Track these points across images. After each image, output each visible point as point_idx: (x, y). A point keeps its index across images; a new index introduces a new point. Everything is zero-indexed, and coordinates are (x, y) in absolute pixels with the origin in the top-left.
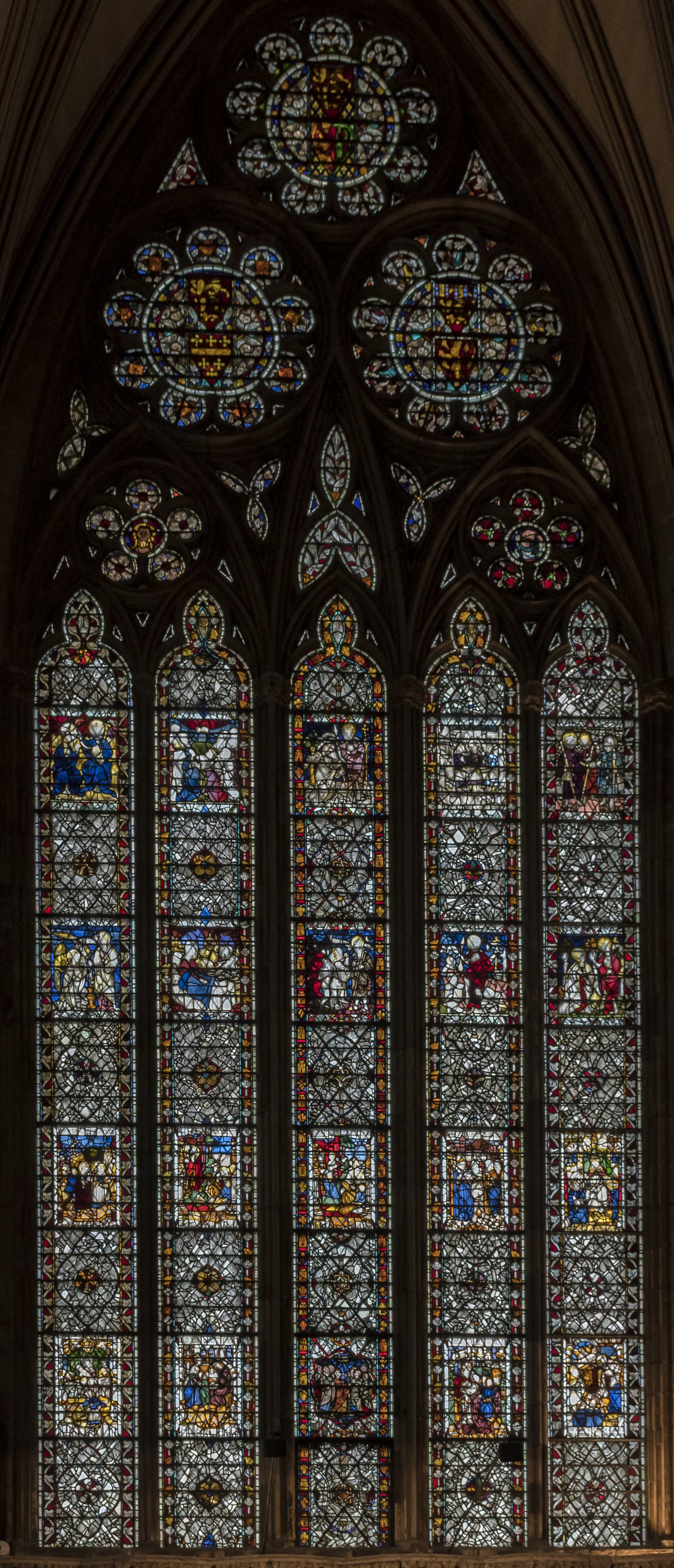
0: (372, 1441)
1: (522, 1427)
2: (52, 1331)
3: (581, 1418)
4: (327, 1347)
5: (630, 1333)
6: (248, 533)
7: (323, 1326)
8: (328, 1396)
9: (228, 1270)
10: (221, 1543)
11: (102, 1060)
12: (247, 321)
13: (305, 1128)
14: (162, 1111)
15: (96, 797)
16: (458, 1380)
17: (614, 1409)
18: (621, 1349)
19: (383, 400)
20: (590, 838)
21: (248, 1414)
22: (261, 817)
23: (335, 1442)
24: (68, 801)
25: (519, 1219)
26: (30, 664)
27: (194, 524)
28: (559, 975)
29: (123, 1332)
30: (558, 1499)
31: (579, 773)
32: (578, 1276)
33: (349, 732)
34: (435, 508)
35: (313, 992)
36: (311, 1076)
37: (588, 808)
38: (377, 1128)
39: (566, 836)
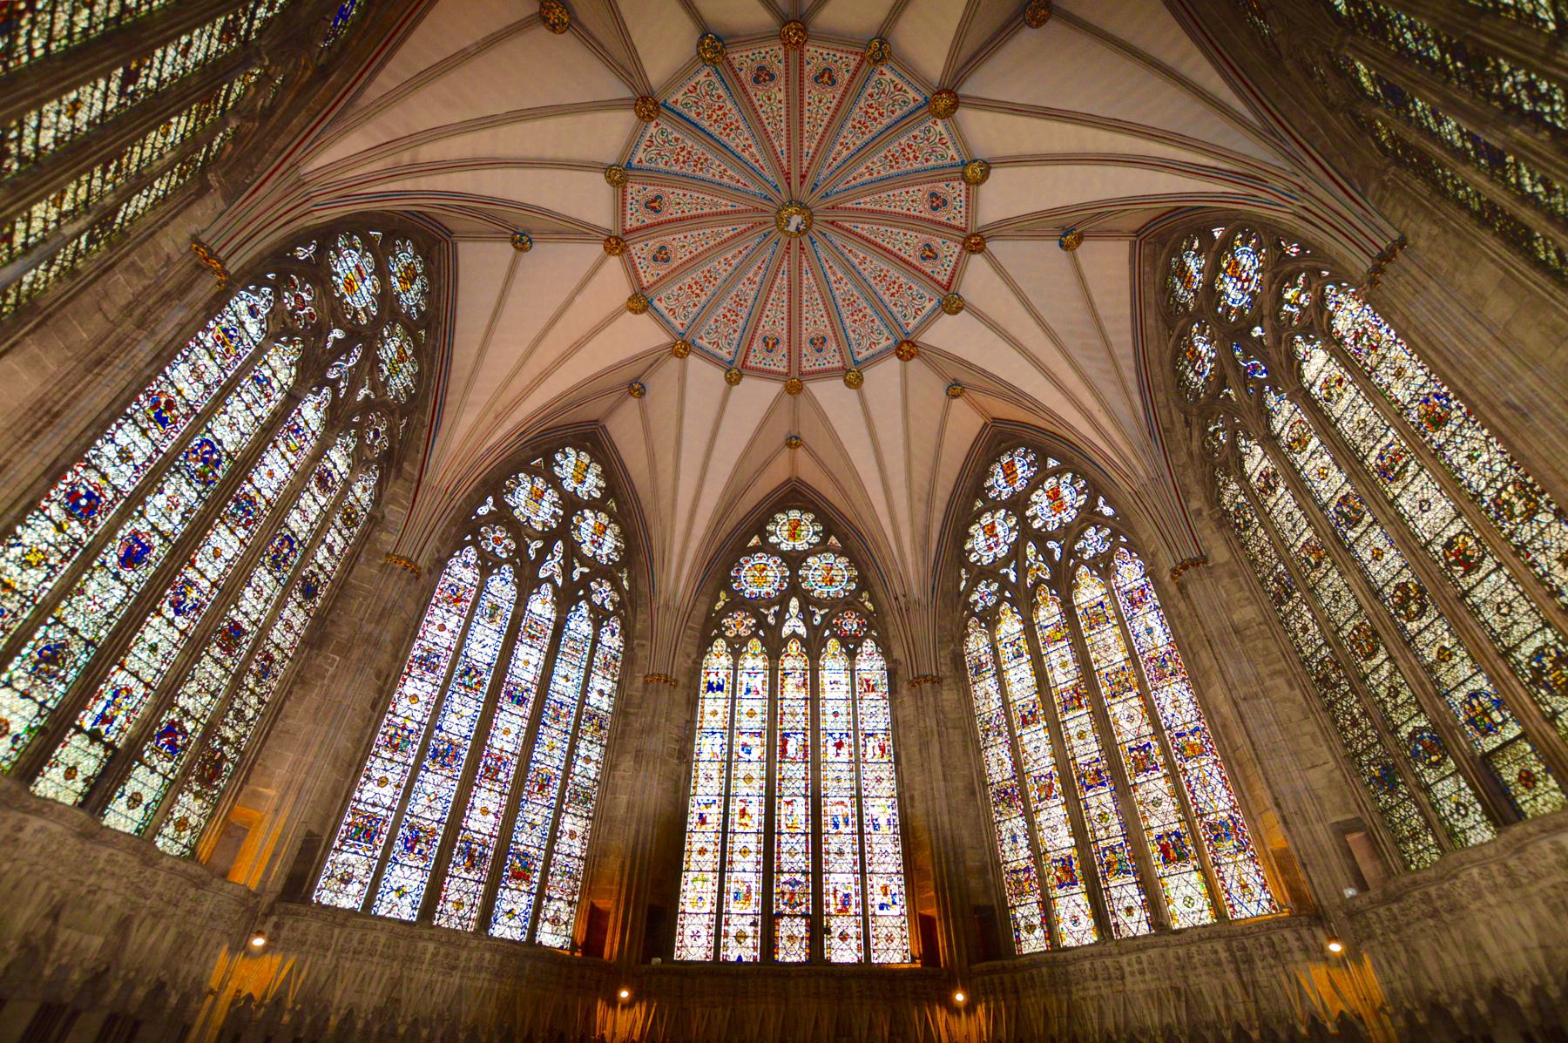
0: (803, 916)
1: (859, 910)
2: (688, 870)
3: (882, 907)
4: (787, 877)
5: (898, 872)
6: (769, 625)
7: (786, 869)
8: (787, 897)
9: (752, 847)
10: (744, 959)
11: (715, 775)
12: (771, 574)
13: (780, 797)
14: (732, 791)
15: (719, 694)
16: (835, 891)
17: (894, 903)
18: (895, 879)
19: (808, 591)
20: (873, 703)
21: (757, 904)
22: (770, 698)
23: (789, 916)
24: (710, 694)
25: (856, 829)
26: (703, 658)
27: (754, 621)
28: (865, 746)
29: (714, 871)
30: (875, 941)
31: (868, 685)
32: (876, 850)
33: (797, 675)
34: (823, 617)
35: (784, 751)
36: (783, 779)
37: (872, 695)
38: (806, 797)
39: (865, 703)
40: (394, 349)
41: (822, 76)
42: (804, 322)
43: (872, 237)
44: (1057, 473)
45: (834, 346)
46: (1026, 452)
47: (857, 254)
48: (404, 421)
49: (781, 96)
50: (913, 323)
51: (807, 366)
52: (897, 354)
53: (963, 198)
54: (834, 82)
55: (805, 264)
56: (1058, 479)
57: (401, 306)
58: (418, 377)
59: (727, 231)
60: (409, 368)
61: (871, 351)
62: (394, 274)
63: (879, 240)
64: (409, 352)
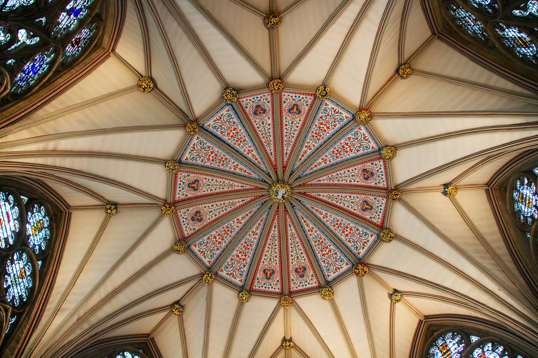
40: (18, 269)
41: (293, 109)
42: (291, 258)
43: (330, 200)
44: (480, 344)
45: (312, 273)
46: (453, 335)
47: (322, 212)
48: (14, 320)
49: (270, 121)
50: (362, 252)
51: (294, 287)
52: (355, 272)
53: (383, 170)
54: (300, 112)
55: (289, 220)
56: (483, 349)
57: (29, 243)
58: (31, 291)
59: (238, 202)
60: (26, 283)
61: (337, 274)
62: (30, 223)
63: (334, 202)
64: (28, 273)
